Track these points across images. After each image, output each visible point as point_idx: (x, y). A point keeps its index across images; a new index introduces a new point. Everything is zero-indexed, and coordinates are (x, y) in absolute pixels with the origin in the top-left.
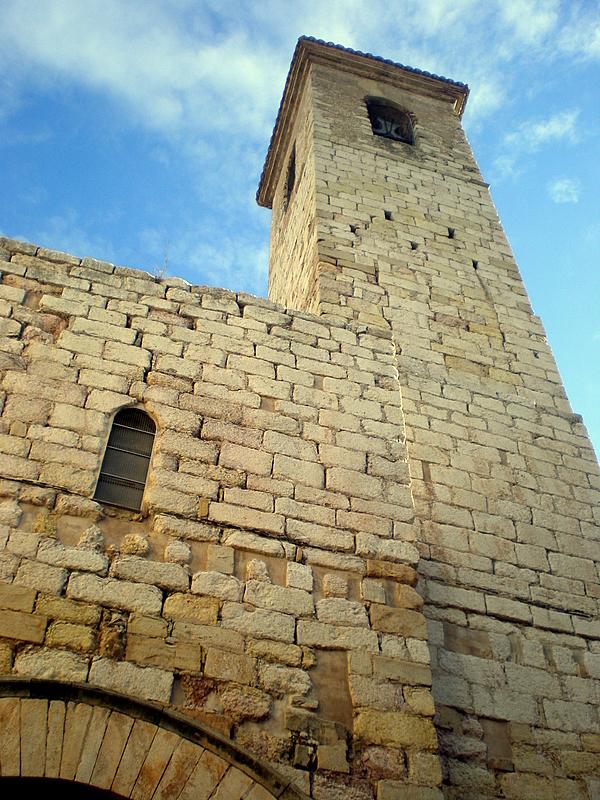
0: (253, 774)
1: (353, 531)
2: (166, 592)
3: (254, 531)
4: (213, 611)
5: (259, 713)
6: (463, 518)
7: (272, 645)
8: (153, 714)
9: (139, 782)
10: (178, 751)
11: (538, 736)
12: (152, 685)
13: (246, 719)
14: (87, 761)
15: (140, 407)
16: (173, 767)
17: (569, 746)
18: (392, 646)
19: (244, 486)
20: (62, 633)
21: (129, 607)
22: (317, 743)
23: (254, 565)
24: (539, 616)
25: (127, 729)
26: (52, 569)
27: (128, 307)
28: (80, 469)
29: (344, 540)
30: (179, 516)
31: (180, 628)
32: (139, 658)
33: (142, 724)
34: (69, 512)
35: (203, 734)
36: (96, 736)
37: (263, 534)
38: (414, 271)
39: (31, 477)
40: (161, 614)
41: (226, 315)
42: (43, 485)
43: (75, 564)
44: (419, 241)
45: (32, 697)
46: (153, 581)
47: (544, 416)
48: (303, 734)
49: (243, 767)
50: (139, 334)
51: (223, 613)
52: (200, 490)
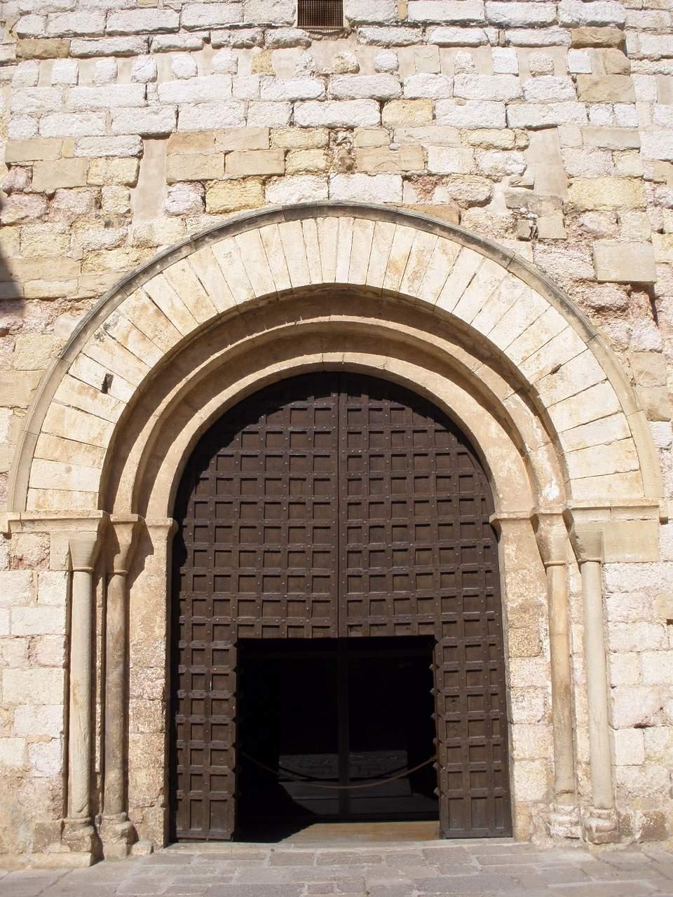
0: (483, 251)
2: (382, 102)
3: (453, 23)
5: (482, 198)
7: (486, 133)
8: (393, 215)
9: (388, 273)
10: (416, 243)
16: (413, 257)
18: (600, 115)
20: (300, 160)
21: (351, 123)
22: (536, 216)
25: (370, 231)
26: (277, 104)
30: (380, 24)
31: (400, 133)
32: (369, 168)
34: (279, 45)
35: (435, 224)
36: (346, 242)
37: (464, 24)
39: (236, 20)
42: (250, 26)
43: (295, 95)
45: (287, 220)
46: (368, 93)
48: (523, 210)
49: (474, 246)
51: (437, 112)
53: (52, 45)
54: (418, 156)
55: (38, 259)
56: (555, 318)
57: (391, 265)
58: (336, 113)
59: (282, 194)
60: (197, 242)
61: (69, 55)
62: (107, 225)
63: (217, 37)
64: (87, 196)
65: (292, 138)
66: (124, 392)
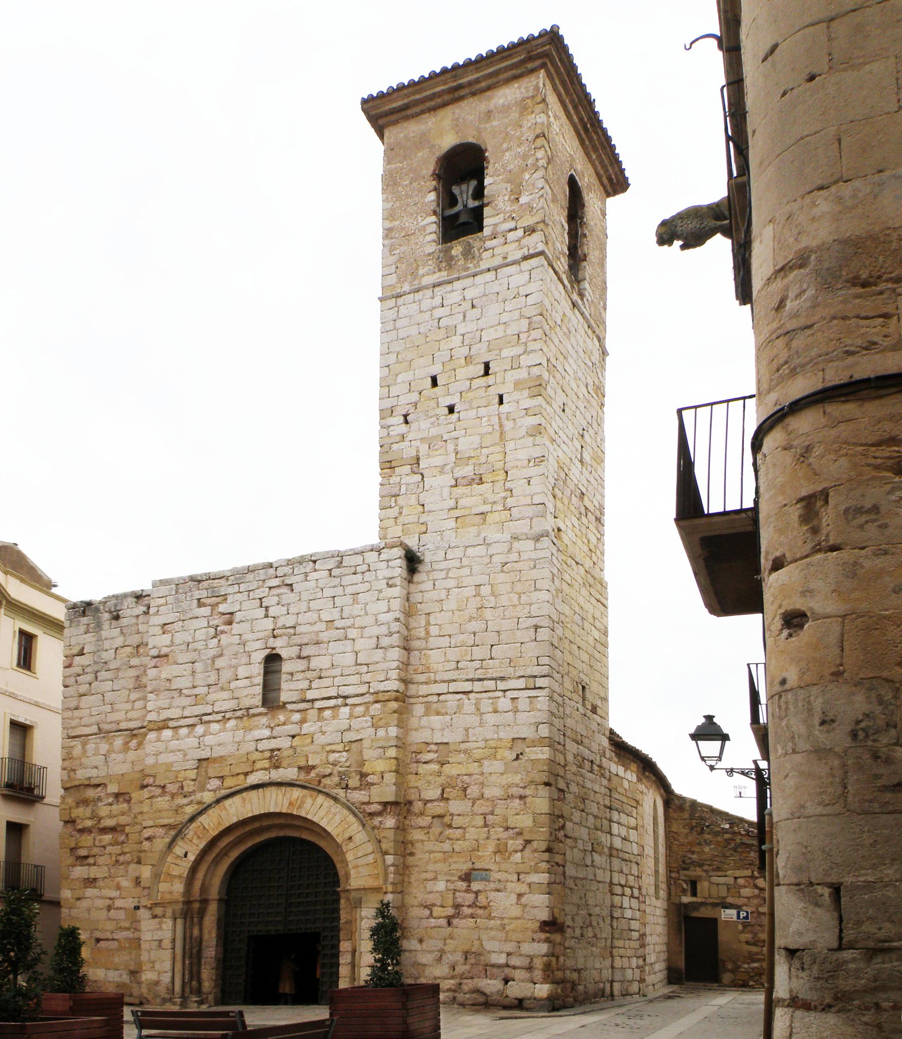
1: (369, 683)
2: (293, 737)
4: (309, 740)
6: (445, 641)
8: (291, 785)
11: (463, 746)
12: (290, 774)
13: (325, 776)
14: (272, 804)
15: (274, 652)
17: (478, 748)
19: (320, 678)
20: (259, 765)
23: (327, 713)
24: (478, 686)
27: (259, 593)
28: (253, 695)
29: (363, 689)
30: (294, 703)
33: (288, 789)
34: (254, 715)
36: (274, 796)
38: (445, 441)
40: (292, 747)
41: (306, 574)
44: (454, 400)
47: (516, 545)
50: (267, 608)
52: (301, 687)
53: (161, 724)
54: (305, 759)
55: (160, 811)
56: (351, 818)
57: (291, 804)
58: (273, 744)
59: (253, 779)
60: (218, 801)
61: (168, 728)
62: (185, 797)
63: (228, 715)
64: (177, 785)
65: (257, 756)
66: (192, 857)
